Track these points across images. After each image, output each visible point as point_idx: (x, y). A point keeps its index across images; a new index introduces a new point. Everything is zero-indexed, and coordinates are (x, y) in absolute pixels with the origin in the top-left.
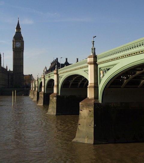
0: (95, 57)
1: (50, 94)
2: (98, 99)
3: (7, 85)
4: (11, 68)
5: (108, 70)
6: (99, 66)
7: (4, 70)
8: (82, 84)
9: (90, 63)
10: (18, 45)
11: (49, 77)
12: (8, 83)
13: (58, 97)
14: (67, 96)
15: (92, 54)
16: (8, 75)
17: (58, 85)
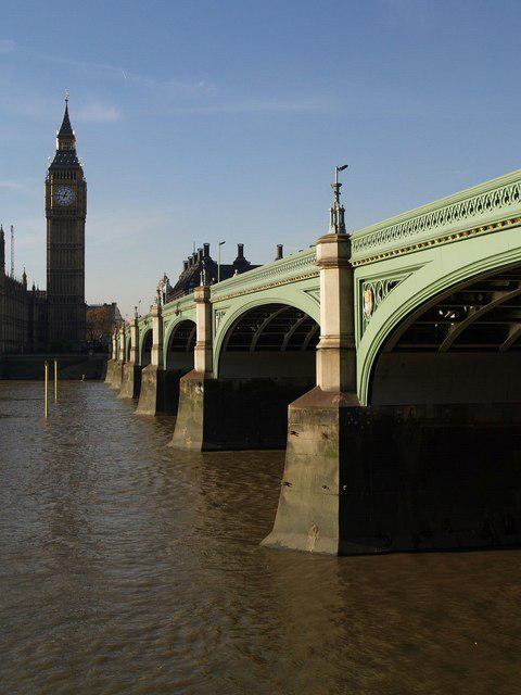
0: (344, 241)
1: (182, 373)
2: (355, 391)
3: (26, 340)
4: (38, 280)
5: (392, 286)
6: (359, 274)
7: (16, 289)
8: (297, 340)
9: (327, 264)
10: (66, 197)
11: (177, 313)
12: (30, 335)
13: (208, 384)
14: (244, 382)
15: (332, 230)
16: (31, 306)
17: (209, 343)
